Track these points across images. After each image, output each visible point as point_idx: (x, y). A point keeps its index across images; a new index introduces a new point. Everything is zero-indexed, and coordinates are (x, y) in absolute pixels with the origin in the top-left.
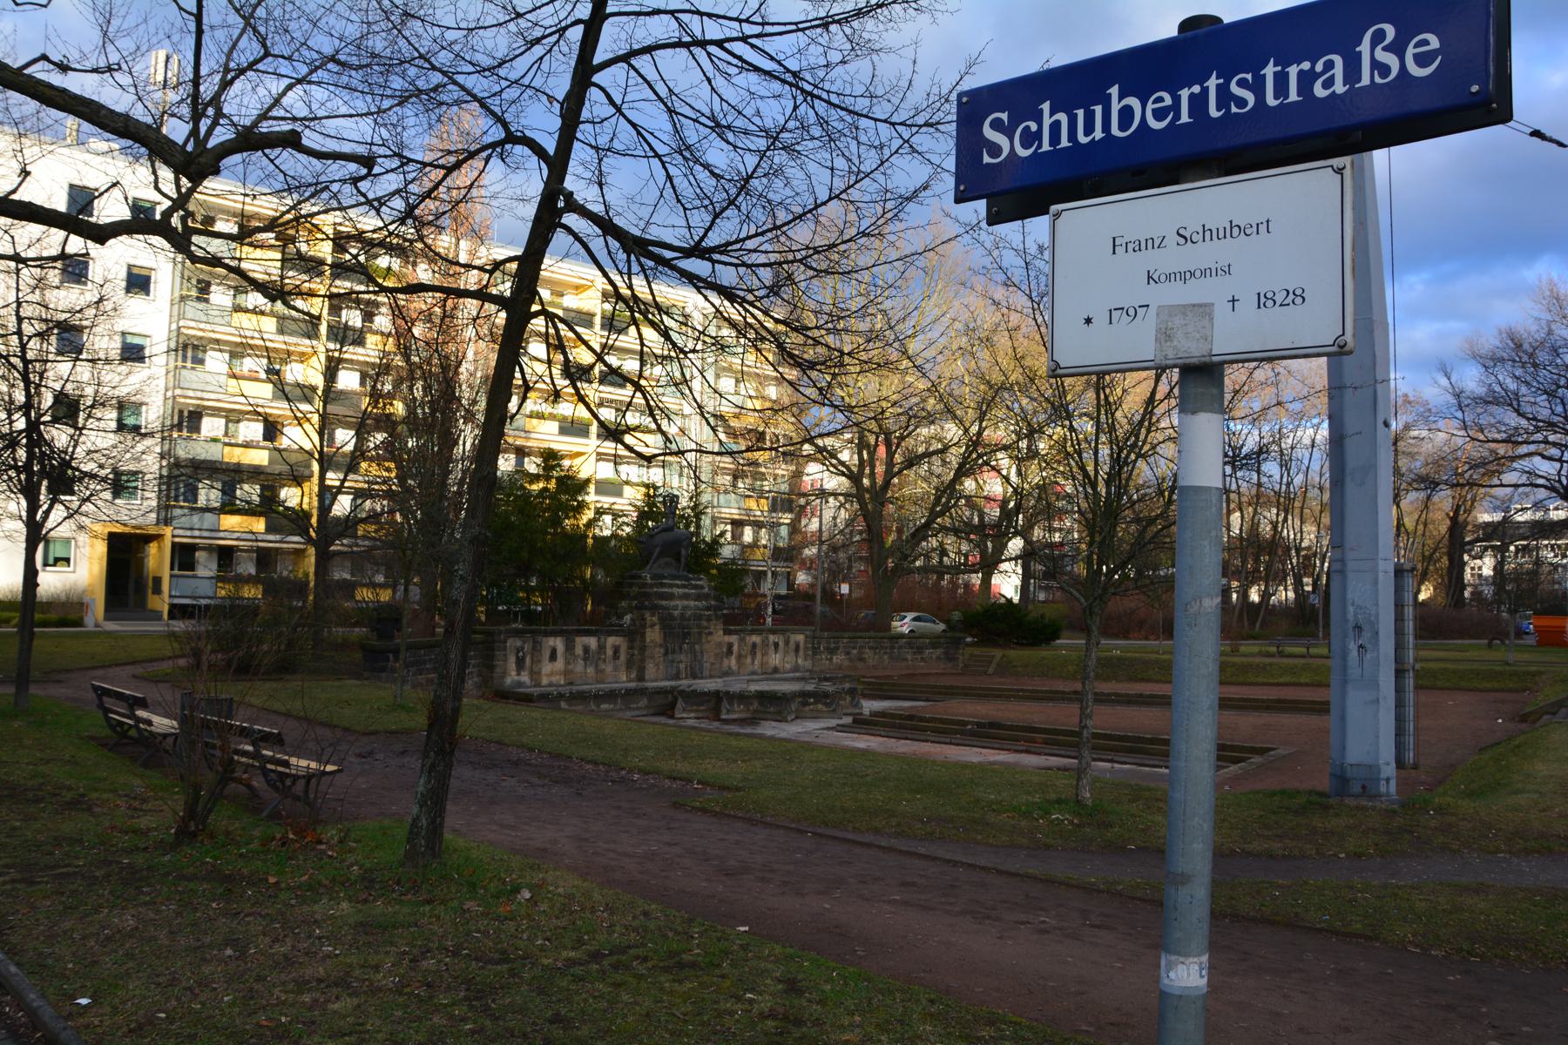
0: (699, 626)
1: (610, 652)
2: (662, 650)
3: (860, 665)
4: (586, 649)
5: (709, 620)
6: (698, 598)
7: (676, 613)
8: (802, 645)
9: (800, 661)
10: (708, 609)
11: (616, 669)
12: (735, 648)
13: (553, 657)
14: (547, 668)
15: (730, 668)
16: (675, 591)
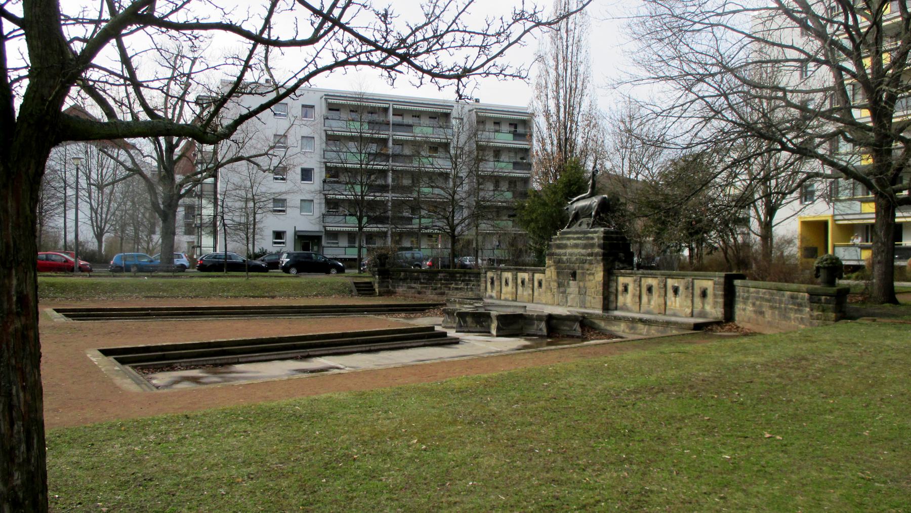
0: (583, 269)
1: (536, 284)
2: (556, 284)
3: (760, 318)
4: (523, 282)
5: (591, 263)
6: (585, 247)
7: (565, 258)
8: (710, 292)
9: (708, 308)
10: (589, 255)
11: (540, 295)
12: (630, 288)
13: (507, 284)
14: (504, 289)
15: (625, 304)
16: (568, 242)
